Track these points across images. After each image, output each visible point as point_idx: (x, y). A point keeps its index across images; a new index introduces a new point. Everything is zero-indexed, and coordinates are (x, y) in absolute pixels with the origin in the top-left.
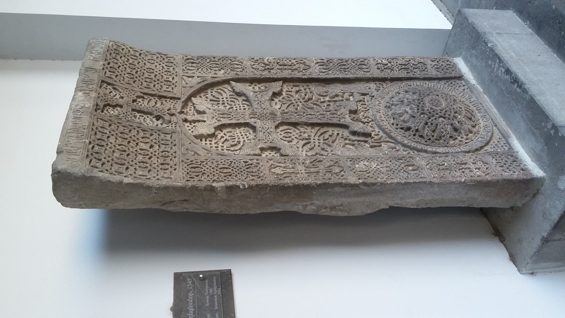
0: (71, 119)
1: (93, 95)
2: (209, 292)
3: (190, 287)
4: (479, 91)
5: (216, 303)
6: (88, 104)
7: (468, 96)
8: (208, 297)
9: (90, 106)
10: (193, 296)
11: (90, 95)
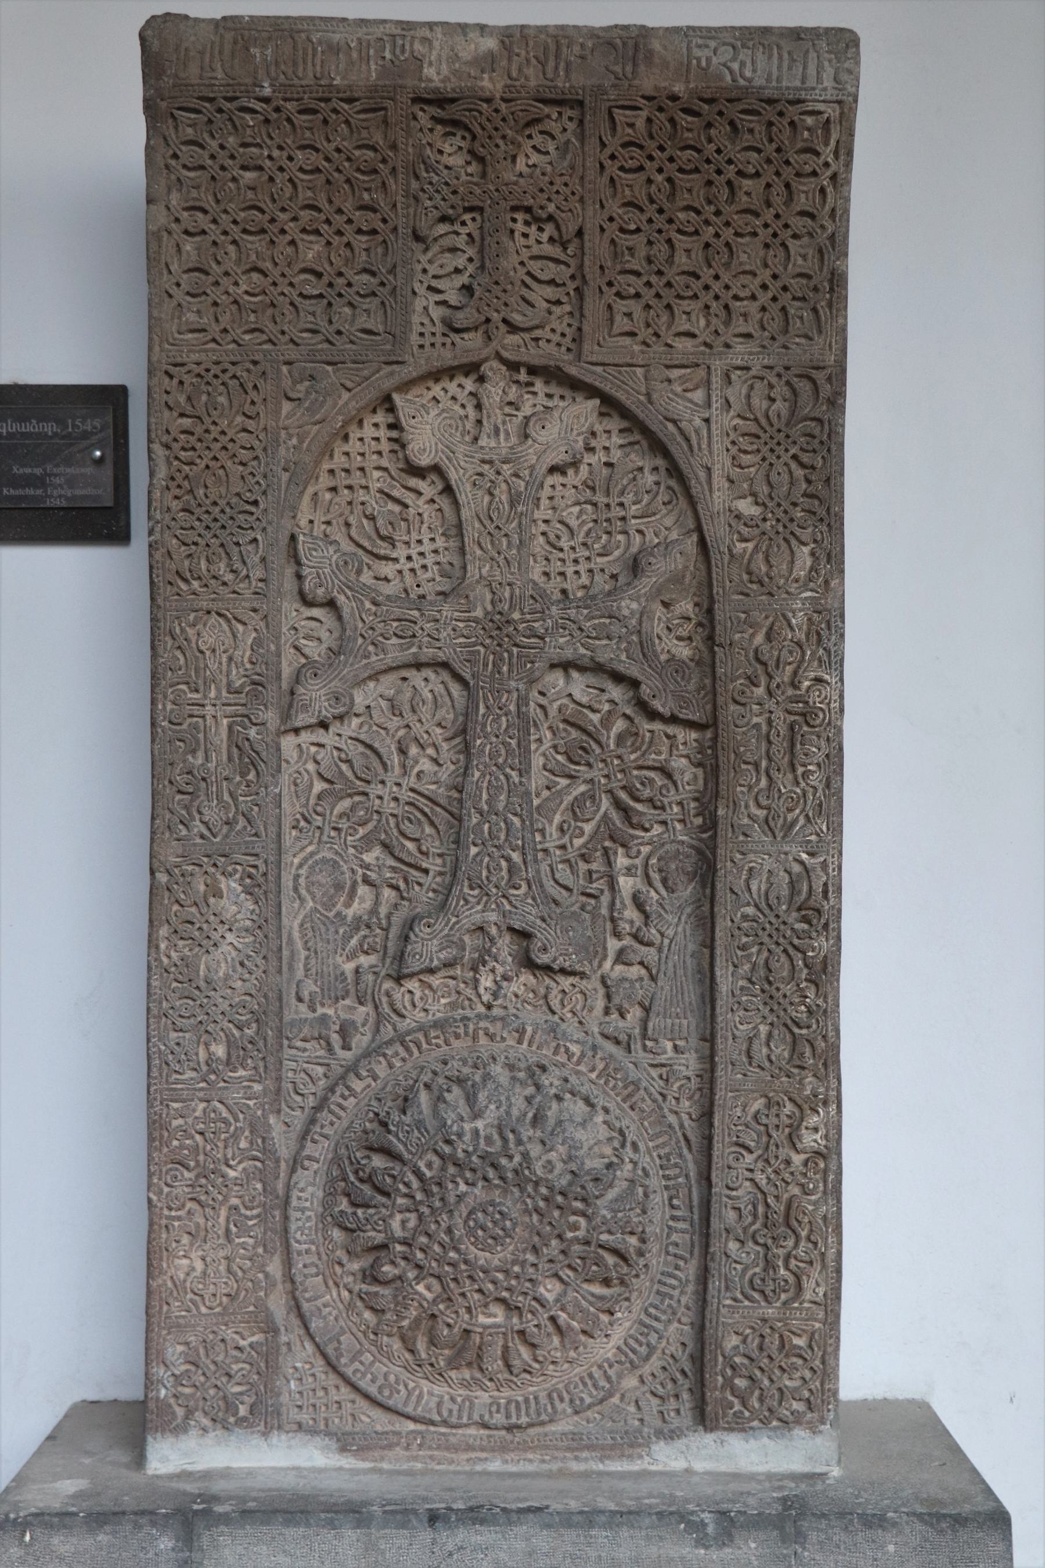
0: (379, 31)
1: (490, 84)
2: (56, 475)
3: (74, 426)
4: (609, 1457)
5: (20, 492)
6: (438, 74)
7: (582, 1400)
8: (38, 471)
9: (431, 80)
10: (46, 434)
11: (485, 76)
